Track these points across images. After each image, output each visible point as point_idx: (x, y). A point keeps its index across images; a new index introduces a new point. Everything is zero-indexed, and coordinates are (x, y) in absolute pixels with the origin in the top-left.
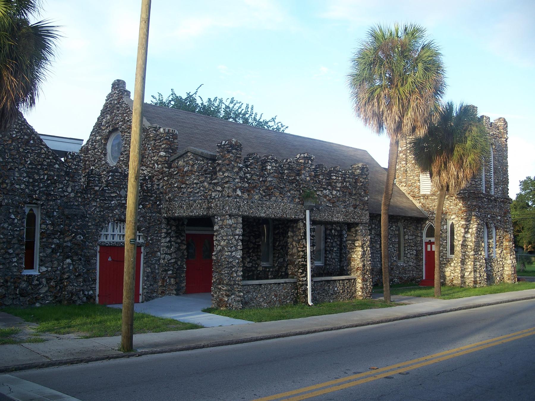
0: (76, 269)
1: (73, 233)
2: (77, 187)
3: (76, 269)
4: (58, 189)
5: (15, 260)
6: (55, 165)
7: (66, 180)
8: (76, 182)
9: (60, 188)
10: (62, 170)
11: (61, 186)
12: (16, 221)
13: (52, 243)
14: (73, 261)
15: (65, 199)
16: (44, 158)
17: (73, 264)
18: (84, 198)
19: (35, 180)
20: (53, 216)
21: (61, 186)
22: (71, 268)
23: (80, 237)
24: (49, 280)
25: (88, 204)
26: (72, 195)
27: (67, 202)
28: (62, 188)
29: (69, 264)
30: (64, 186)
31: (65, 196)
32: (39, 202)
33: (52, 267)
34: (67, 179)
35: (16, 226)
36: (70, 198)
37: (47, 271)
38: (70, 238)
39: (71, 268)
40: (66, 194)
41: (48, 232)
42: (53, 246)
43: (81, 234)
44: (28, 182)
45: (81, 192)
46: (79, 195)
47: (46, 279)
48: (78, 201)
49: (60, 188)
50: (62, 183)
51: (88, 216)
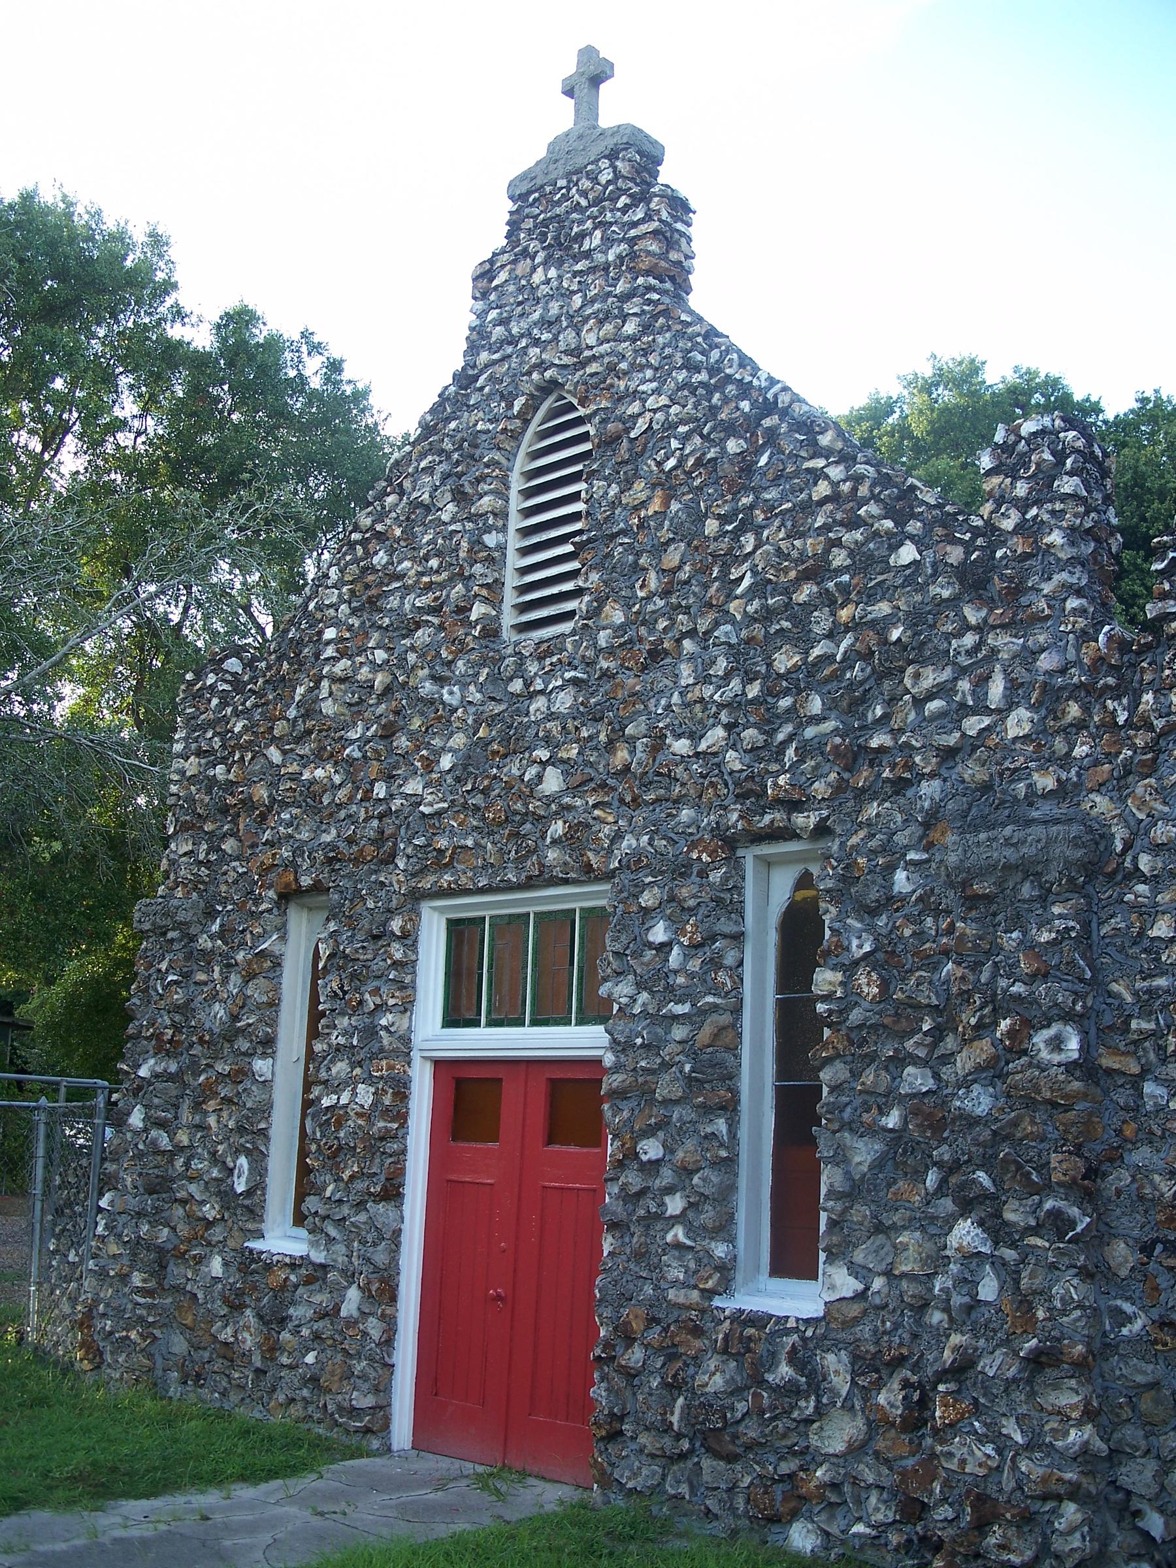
0: (1025, 1304)
1: (998, 1006)
2: (1046, 662)
3: (1025, 1304)
4: (918, 703)
5: (675, 1205)
6: (895, 548)
7: (967, 627)
8: (1039, 619)
9: (930, 696)
10: (940, 566)
11: (931, 678)
12: (675, 957)
13: (886, 1100)
14: (996, 1229)
15: (972, 771)
16: (826, 528)
17: (1000, 1264)
18: (1110, 724)
19: (774, 685)
20: (891, 901)
21: (931, 678)
22: (988, 1289)
23: (1057, 1044)
24: (871, 1367)
25: (1151, 768)
26: (1019, 723)
27: (986, 788)
28: (942, 690)
29: (972, 1258)
30: (962, 671)
31: (971, 745)
32: (799, 819)
33: (888, 1274)
34: (973, 615)
35: (672, 993)
36: (1008, 749)
37: (861, 1296)
38: (983, 1050)
39: (988, 1289)
40: (973, 725)
41: (855, 1016)
42: (892, 1120)
43: (1068, 1017)
44: (736, 704)
45: (1088, 693)
46: (1074, 710)
47: (855, 1358)
48: (1066, 761)
49: (930, 696)
50: (941, 658)
51: (1145, 863)
